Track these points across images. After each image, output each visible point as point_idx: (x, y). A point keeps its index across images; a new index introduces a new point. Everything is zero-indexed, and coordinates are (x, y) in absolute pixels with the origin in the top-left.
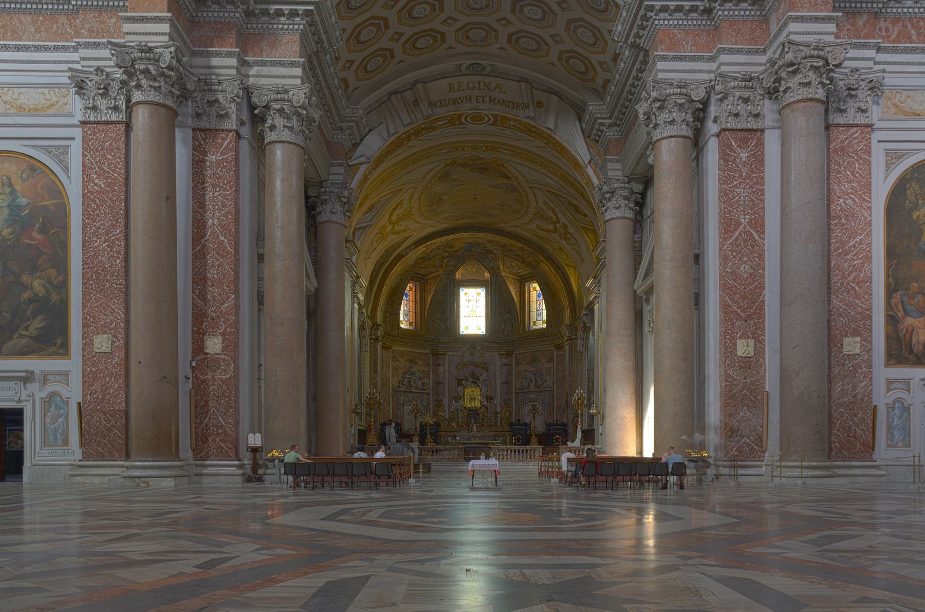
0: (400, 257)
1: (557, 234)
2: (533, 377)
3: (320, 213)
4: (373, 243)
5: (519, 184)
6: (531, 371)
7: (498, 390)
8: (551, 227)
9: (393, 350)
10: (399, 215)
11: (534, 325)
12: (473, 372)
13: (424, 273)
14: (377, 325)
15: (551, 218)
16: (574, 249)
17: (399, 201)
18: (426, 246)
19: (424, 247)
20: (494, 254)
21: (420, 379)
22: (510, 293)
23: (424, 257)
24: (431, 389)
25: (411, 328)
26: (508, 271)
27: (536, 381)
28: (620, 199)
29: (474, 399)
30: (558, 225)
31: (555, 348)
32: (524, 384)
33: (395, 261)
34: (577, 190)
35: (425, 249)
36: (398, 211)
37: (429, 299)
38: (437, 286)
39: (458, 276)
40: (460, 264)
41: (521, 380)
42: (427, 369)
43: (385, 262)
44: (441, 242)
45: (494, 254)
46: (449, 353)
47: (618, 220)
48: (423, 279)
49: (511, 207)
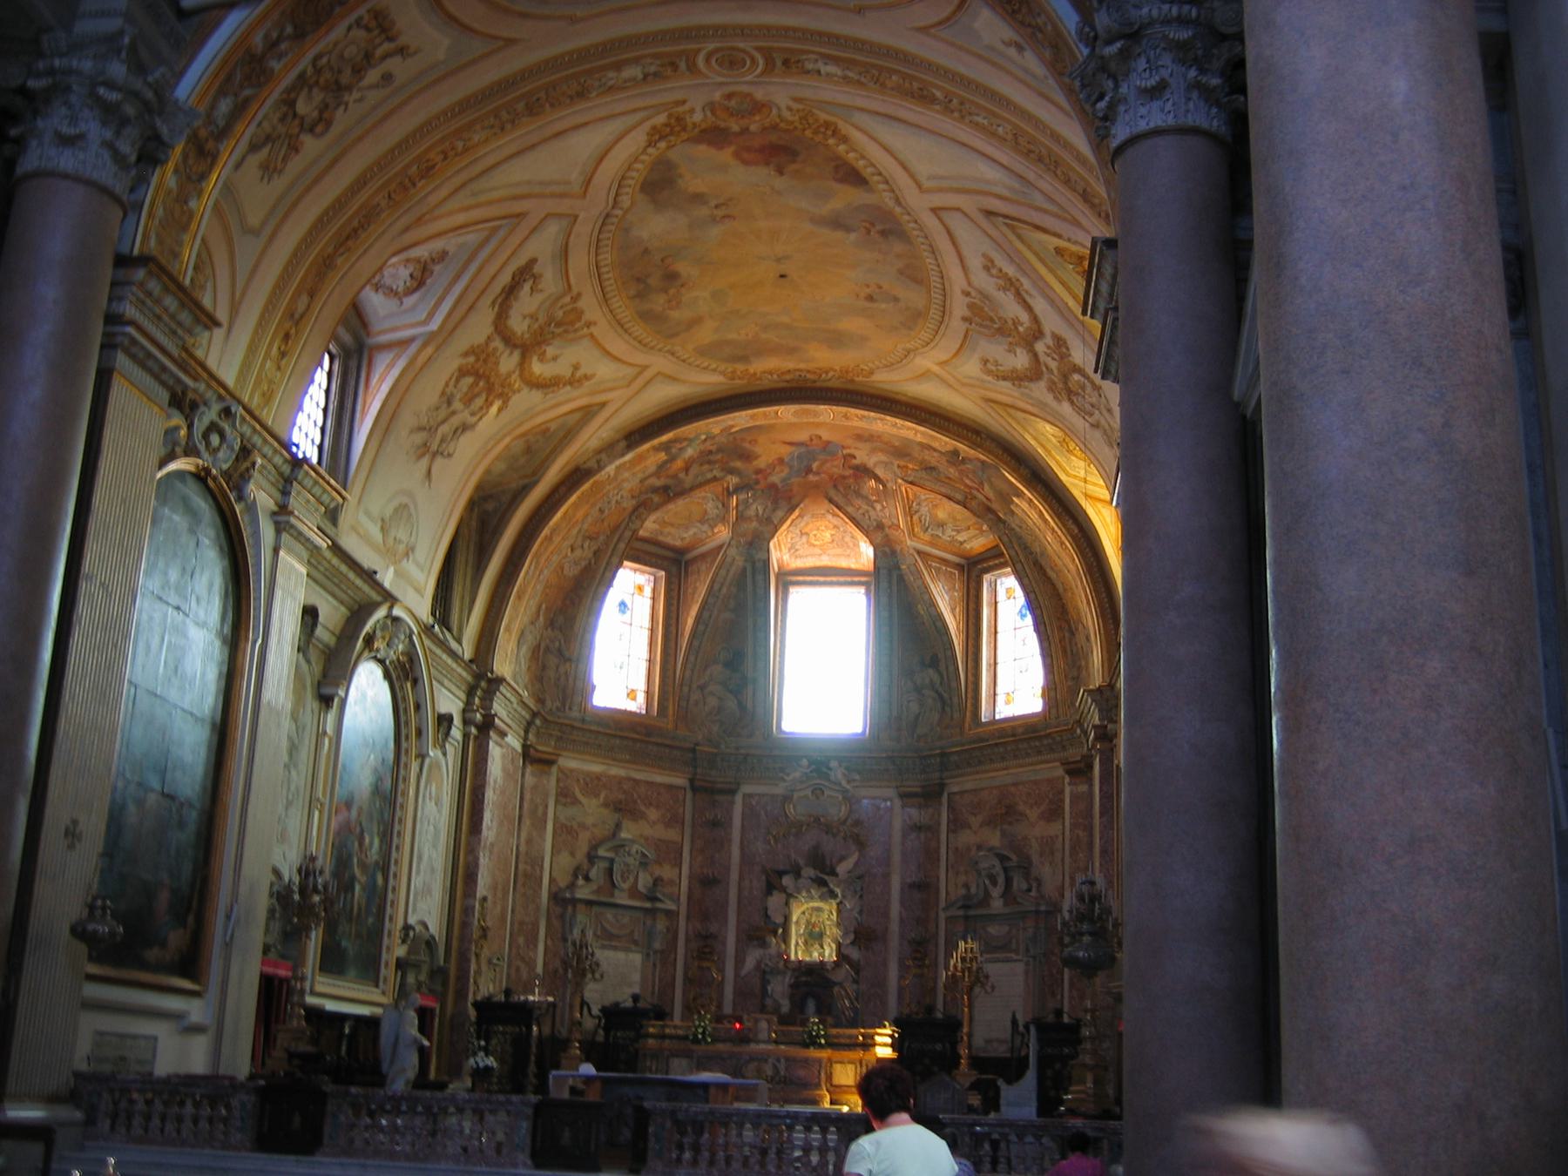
0: (576, 477)
1: (1042, 384)
2: (997, 862)
3: (20, 142)
4: (449, 403)
5: (898, 202)
6: (991, 849)
7: (895, 909)
8: (1021, 360)
9: (561, 770)
10: (533, 317)
11: (1007, 702)
12: (816, 847)
13: (678, 543)
14: (490, 681)
15: (1016, 322)
16: (1096, 426)
17: (520, 261)
18: (666, 447)
19: (657, 449)
20: (878, 479)
21: (644, 864)
22: (933, 604)
23: (666, 489)
24: (684, 898)
25: (637, 705)
26: (927, 537)
27: (1008, 881)
28: (1167, 59)
29: (821, 936)
30: (1040, 347)
31: (1069, 772)
32: (973, 890)
33: (563, 490)
34: (1067, 182)
35: (662, 456)
36: (527, 303)
37: (690, 622)
38: (713, 581)
39: (783, 552)
40: (780, 513)
41: (962, 879)
42: (672, 834)
43: (524, 490)
44: (710, 437)
45: (878, 479)
46: (747, 789)
47: (1160, 141)
48: (677, 562)
49: (896, 299)
